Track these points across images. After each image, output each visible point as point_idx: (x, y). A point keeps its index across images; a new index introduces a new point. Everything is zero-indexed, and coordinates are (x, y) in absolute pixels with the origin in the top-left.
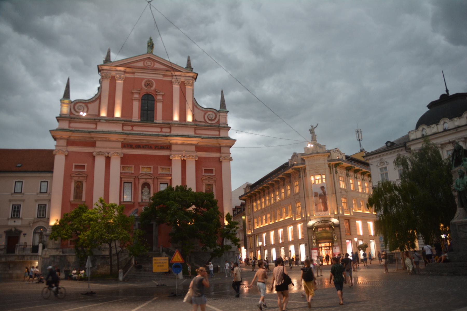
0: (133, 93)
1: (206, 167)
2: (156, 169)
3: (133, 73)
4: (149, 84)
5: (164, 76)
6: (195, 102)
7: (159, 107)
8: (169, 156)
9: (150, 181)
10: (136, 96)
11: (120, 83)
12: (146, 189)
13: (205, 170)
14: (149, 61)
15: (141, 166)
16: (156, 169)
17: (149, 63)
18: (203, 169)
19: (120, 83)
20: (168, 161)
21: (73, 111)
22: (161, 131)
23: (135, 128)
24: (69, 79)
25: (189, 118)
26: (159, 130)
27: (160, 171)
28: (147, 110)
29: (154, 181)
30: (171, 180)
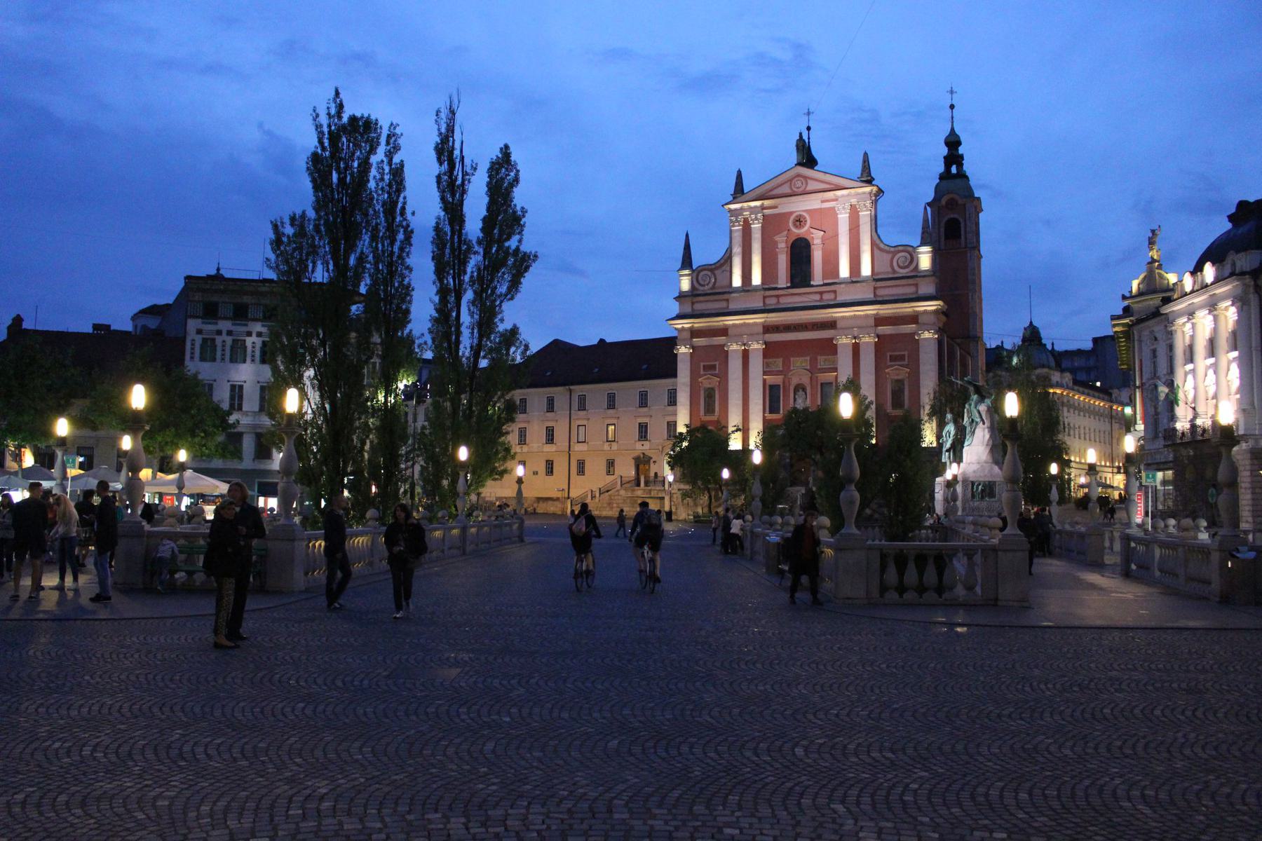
5: (823, 202)
8: (832, 339)
9: (805, 380)
10: (782, 245)
11: (756, 226)
12: (801, 393)
16: (814, 362)
17: (799, 184)
19: (756, 226)
20: (830, 347)
21: (696, 285)
22: (821, 299)
23: (782, 300)
24: (687, 235)
25: (866, 270)
26: (817, 297)
30: (836, 377)
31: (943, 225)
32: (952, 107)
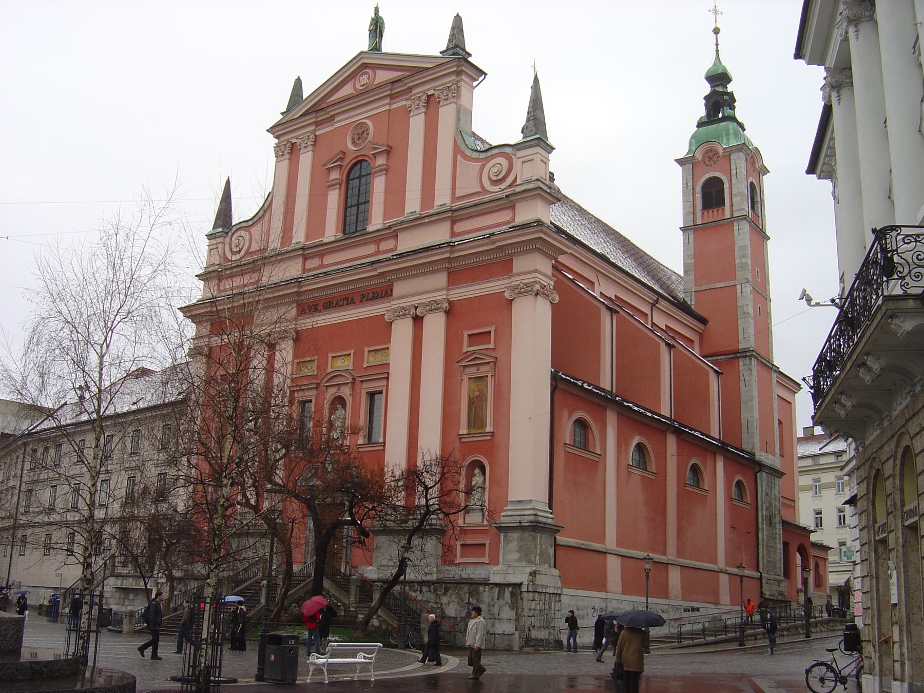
0: (329, 170)
1: (474, 328)
2: (359, 357)
3: (332, 118)
4: (360, 132)
6: (460, 142)
7: (379, 185)
13: (469, 336)
14: (365, 73)
15: (330, 355)
17: (364, 79)
18: (466, 333)
23: (328, 260)
27: (370, 360)
28: (358, 205)
29: (353, 389)
31: (699, 189)
32: (716, 31)
